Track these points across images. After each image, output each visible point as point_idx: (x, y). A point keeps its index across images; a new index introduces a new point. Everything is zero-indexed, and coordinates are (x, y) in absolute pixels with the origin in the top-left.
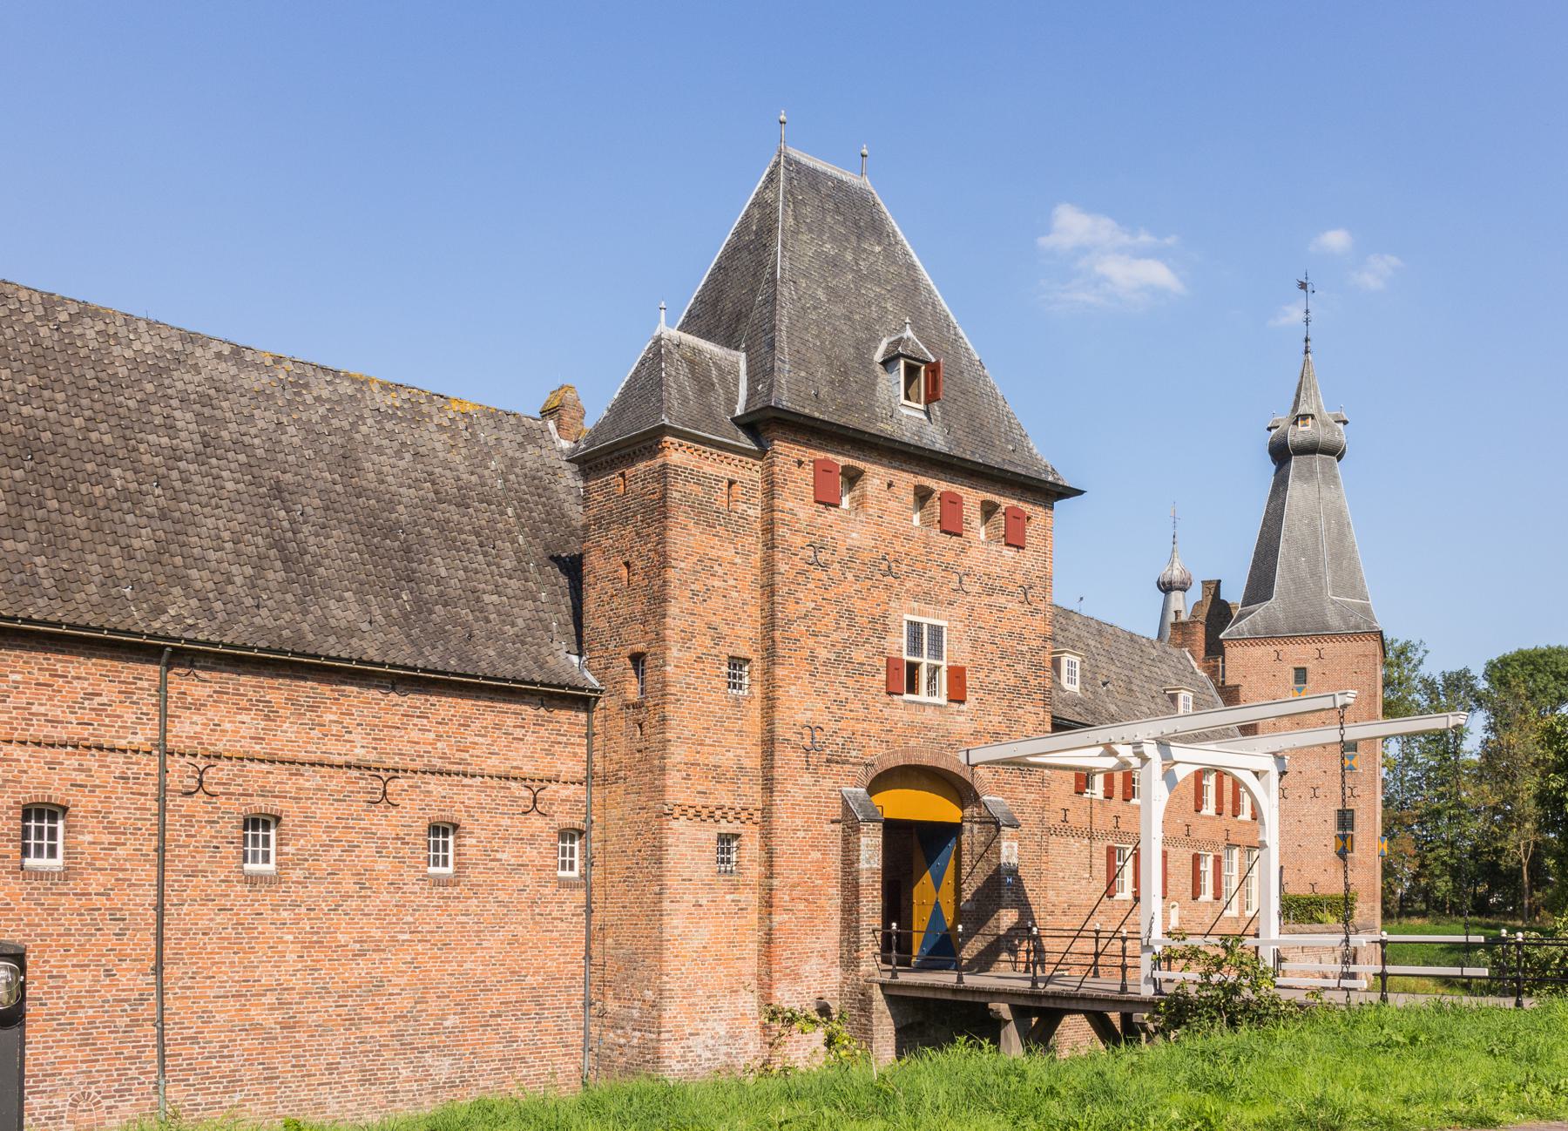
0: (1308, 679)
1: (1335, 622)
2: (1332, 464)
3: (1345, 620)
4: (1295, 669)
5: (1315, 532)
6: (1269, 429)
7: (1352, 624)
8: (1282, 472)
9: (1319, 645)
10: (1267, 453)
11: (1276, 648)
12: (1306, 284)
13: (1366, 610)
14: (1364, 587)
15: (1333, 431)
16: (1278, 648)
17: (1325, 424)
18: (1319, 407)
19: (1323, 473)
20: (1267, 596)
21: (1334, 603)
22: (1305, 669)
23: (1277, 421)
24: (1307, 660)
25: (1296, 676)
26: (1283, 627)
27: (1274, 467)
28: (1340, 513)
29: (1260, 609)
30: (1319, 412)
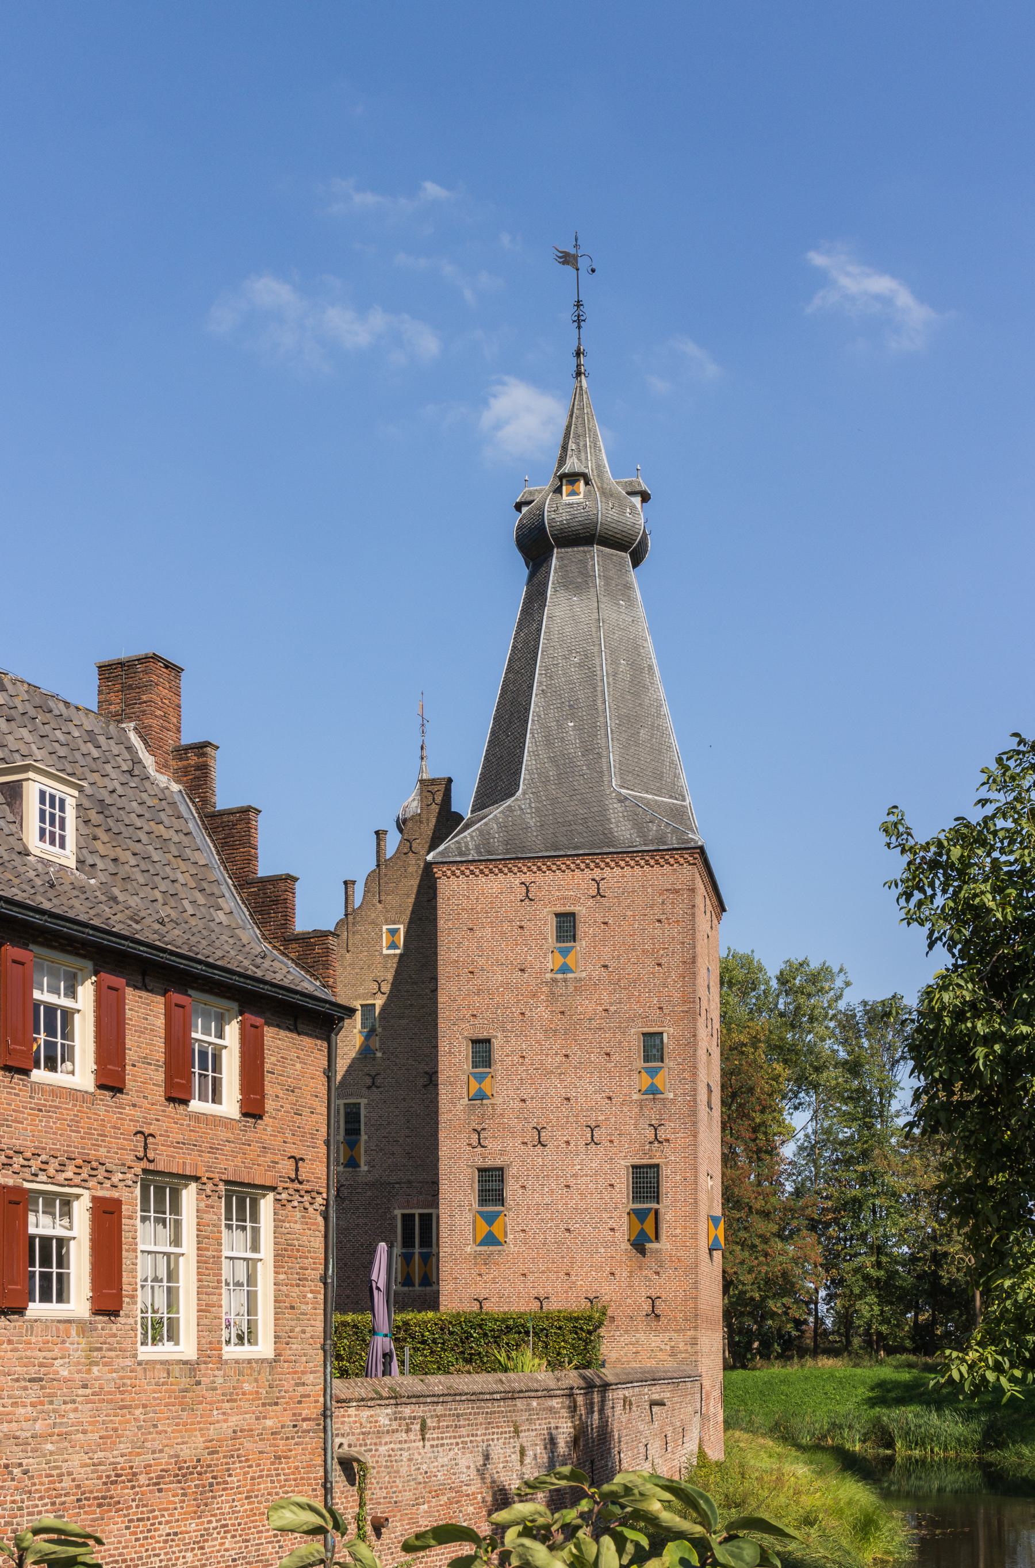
0: (580, 933)
1: (624, 832)
2: (622, 564)
3: (639, 827)
4: (557, 915)
5: (591, 679)
6: (518, 507)
7: (651, 835)
8: (539, 576)
9: (597, 873)
10: (514, 543)
11: (524, 878)
12: (575, 257)
13: (679, 814)
14: (676, 776)
15: (622, 506)
16: (528, 878)
17: (607, 494)
18: (599, 467)
19: (607, 579)
20: (510, 791)
21: (622, 799)
22: (573, 915)
23: (531, 493)
24: (576, 900)
25: (559, 928)
26: (535, 841)
27: (526, 572)
28: (635, 648)
29: (496, 812)
30: (601, 474)
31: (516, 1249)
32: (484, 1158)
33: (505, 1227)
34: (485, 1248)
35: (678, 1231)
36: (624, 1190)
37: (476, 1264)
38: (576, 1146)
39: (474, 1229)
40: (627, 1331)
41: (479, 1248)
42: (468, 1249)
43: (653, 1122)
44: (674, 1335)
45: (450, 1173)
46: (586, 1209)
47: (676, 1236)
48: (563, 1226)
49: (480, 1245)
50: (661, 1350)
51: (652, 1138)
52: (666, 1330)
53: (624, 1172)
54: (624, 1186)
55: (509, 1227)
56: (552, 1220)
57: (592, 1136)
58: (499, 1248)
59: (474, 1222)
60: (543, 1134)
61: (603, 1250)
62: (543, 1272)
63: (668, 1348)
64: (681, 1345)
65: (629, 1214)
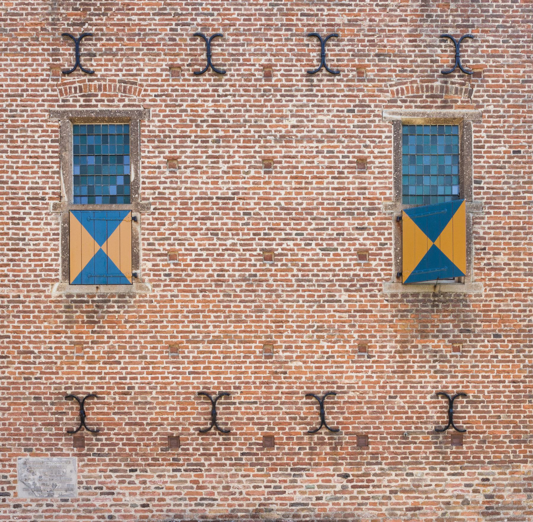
31: (158, 292)
32: (88, 97)
33: (135, 244)
34: (92, 289)
35: (502, 259)
36: (390, 172)
37: (70, 322)
38: (287, 76)
39: (66, 248)
40: (394, 466)
41: (76, 290)
42: (54, 291)
43: (451, 31)
44: (493, 473)
45: (14, 128)
46: (309, 211)
47: (497, 269)
48: (259, 245)
49: (79, 281)
50: (466, 502)
51: (447, 62)
52: (476, 463)
53: (388, 133)
54: (389, 163)
55: (142, 246)
56: (236, 231)
57: (323, 56)
58: (122, 289)
59: (66, 233)
60: (216, 50)
61: (345, 296)
62: (217, 341)
63: (480, 498)
64: (507, 494)
65: (399, 220)
